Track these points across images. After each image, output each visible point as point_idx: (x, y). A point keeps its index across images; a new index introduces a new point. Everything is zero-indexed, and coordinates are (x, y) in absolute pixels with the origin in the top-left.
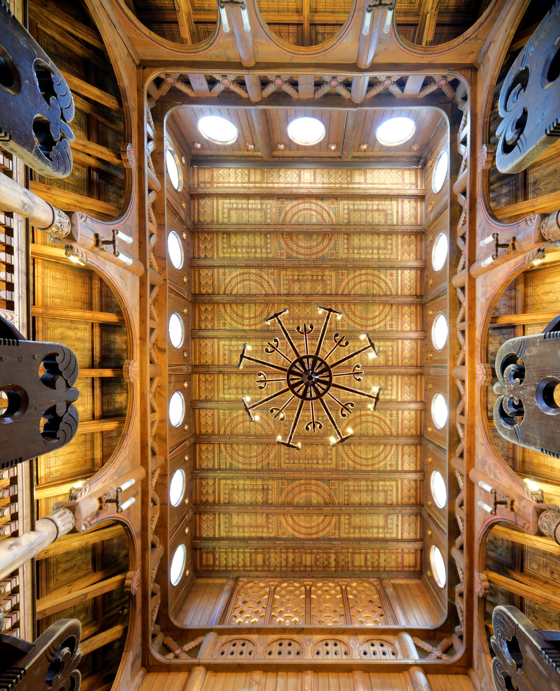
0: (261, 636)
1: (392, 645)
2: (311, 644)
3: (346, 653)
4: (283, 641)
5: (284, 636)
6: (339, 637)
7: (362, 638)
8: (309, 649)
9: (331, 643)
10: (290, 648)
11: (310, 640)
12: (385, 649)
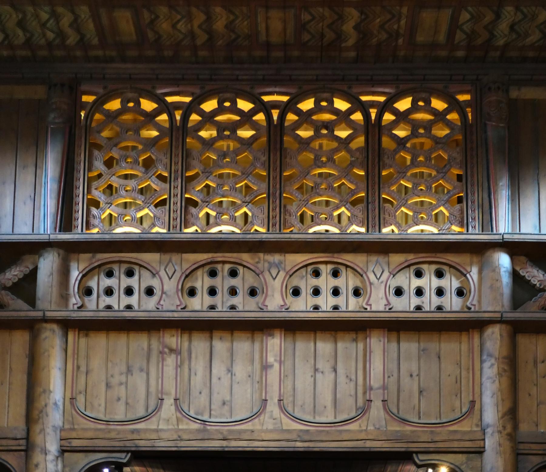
0: (166, 257)
1: (462, 274)
2: (282, 274)
3: (357, 293)
4: (219, 267)
5: (219, 256)
6: (348, 258)
7: (397, 259)
8: (277, 283)
9: (325, 270)
10: (234, 282)
11: (279, 266)
12: (444, 283)
